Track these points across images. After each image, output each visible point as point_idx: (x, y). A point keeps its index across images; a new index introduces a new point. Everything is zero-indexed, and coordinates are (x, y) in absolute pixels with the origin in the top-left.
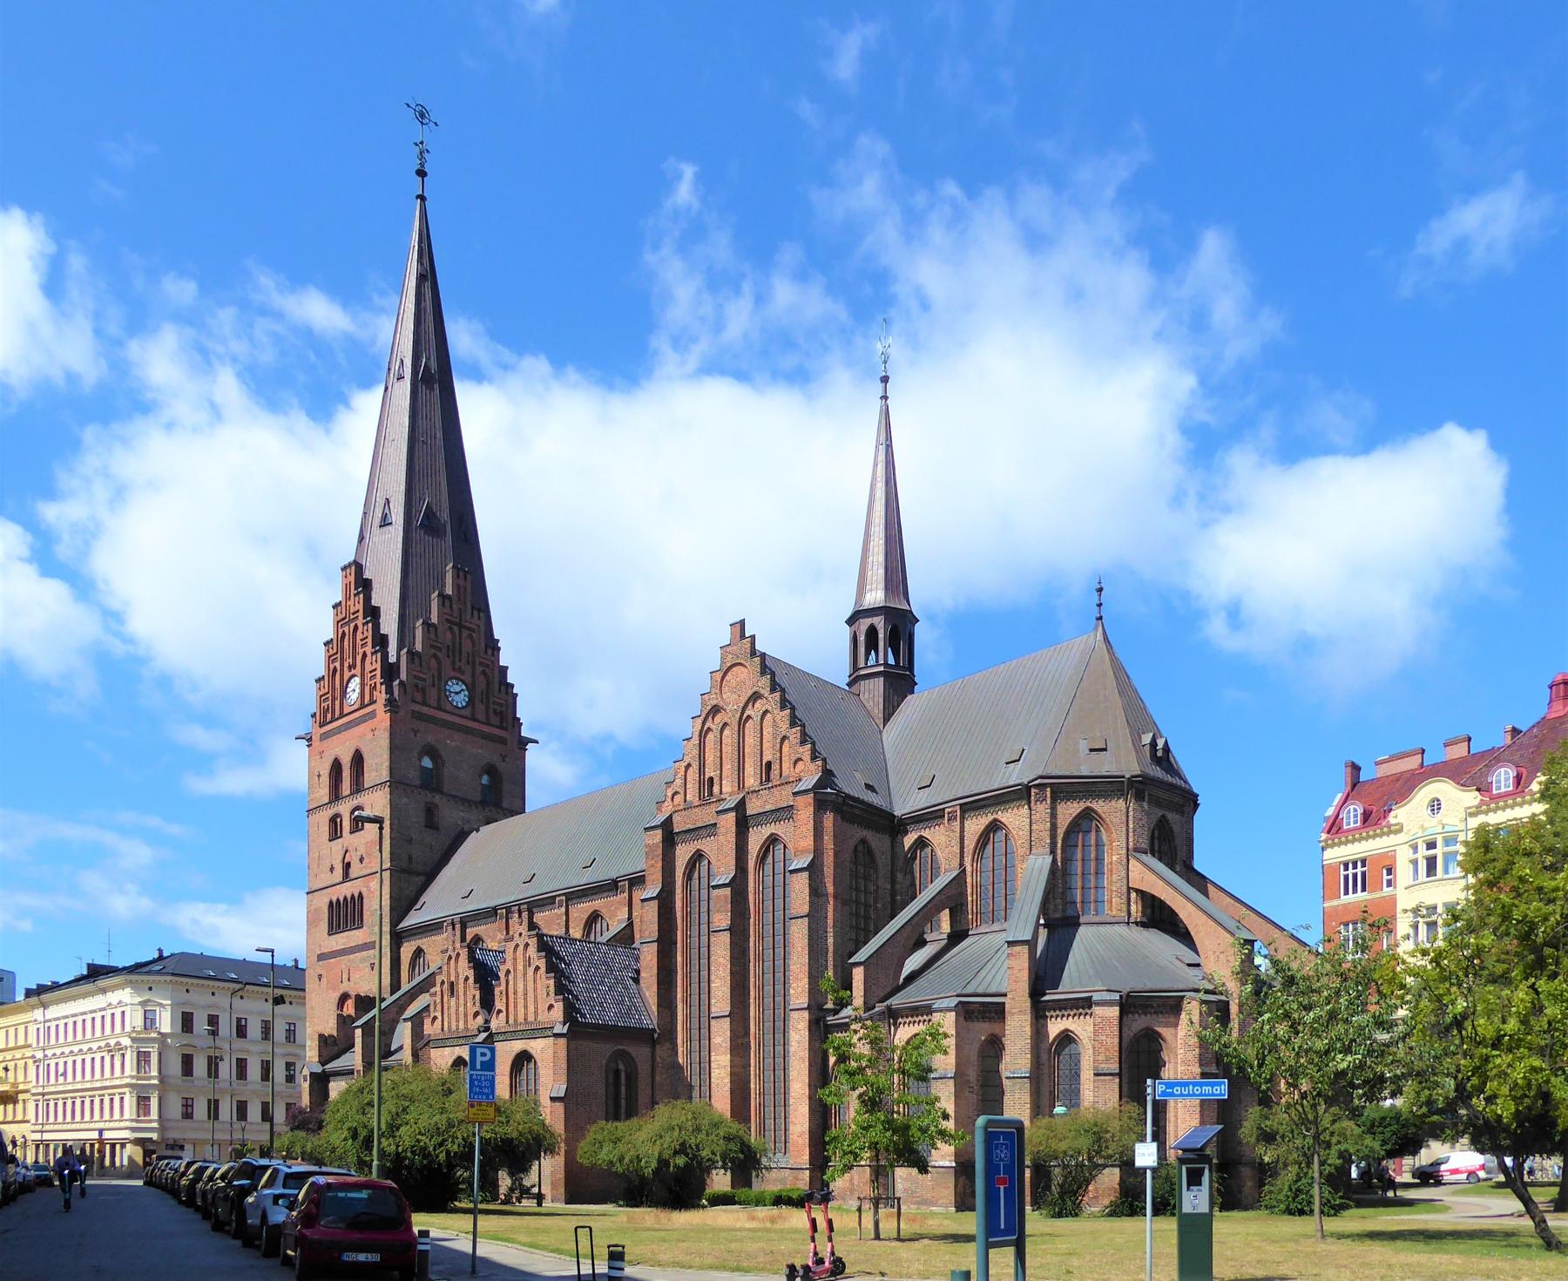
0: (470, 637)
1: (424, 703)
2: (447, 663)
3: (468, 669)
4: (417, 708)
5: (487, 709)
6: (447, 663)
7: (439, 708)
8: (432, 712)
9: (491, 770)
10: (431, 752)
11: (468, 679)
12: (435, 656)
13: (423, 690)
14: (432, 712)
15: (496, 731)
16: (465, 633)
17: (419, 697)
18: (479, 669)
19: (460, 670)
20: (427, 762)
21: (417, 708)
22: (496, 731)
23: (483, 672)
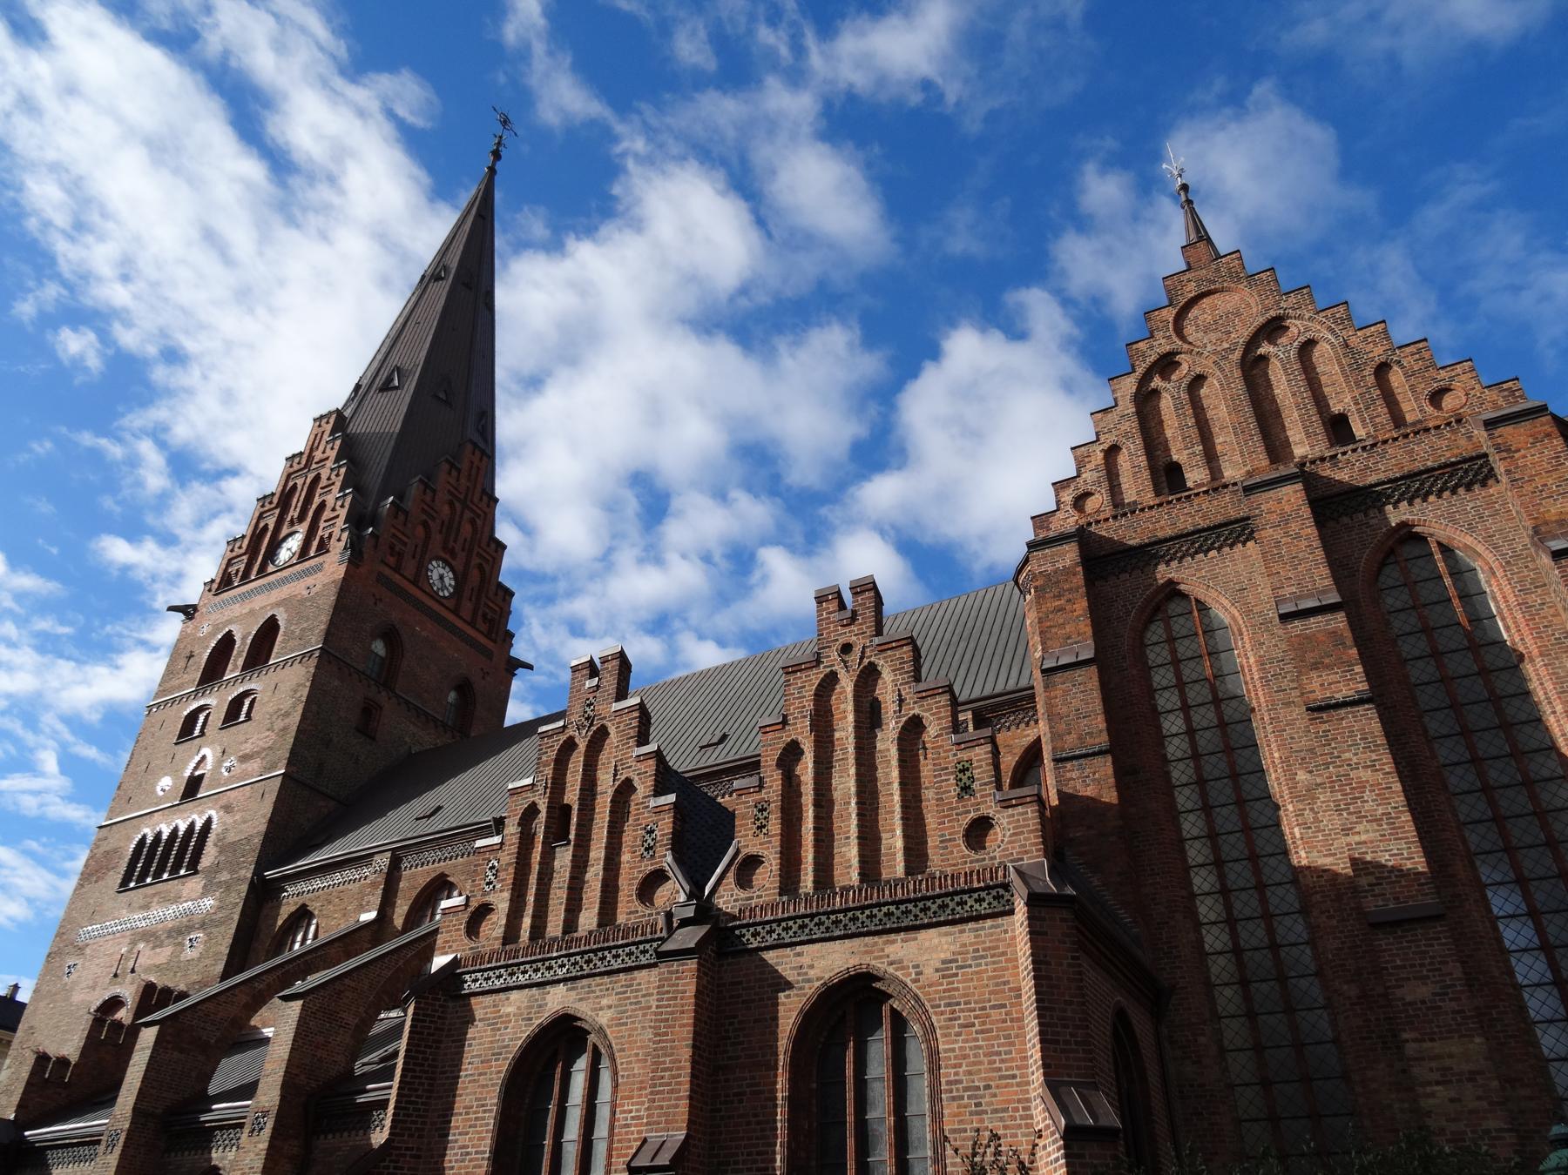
0: (473, 522)
1: (397, 569)
2: (437, 538)
3: (462, 555)
4: (387, 571)
5: (475, 611)
6: (437, 538)
7: (415, 583)
8: (404, 584)
9: (464, 688)
10: (390, 636)
11: (458, 564)
12: (425, 524)
13: (400, 555)
14: (404, 584)
15: (483, 640)
16: (468, 515)
17: (392, 560)
18: (476, 561)
19: (452, 553)
20: (379, 647)
21: (387, 571)
22: (483, 640)
23: (480, 567)
